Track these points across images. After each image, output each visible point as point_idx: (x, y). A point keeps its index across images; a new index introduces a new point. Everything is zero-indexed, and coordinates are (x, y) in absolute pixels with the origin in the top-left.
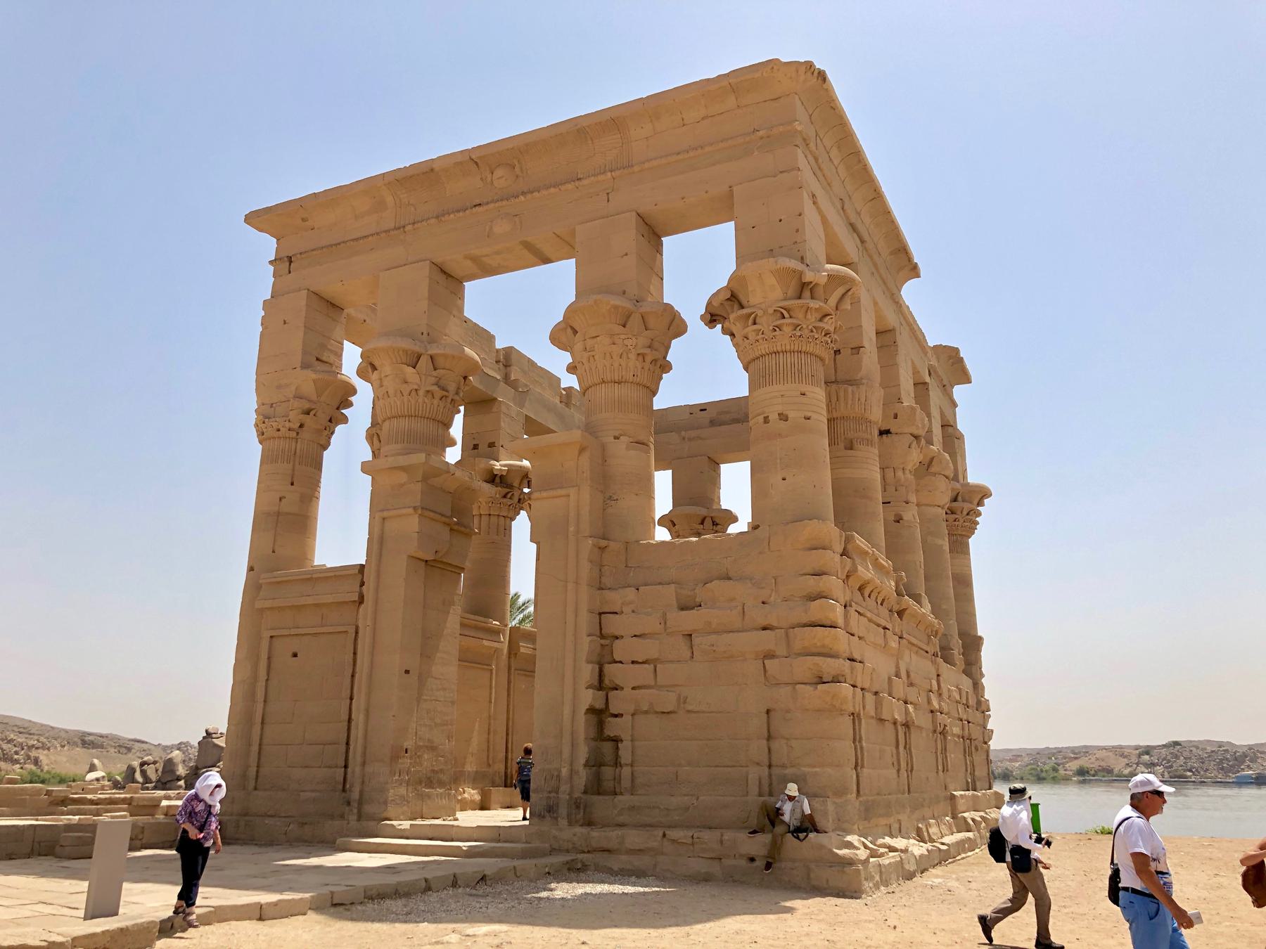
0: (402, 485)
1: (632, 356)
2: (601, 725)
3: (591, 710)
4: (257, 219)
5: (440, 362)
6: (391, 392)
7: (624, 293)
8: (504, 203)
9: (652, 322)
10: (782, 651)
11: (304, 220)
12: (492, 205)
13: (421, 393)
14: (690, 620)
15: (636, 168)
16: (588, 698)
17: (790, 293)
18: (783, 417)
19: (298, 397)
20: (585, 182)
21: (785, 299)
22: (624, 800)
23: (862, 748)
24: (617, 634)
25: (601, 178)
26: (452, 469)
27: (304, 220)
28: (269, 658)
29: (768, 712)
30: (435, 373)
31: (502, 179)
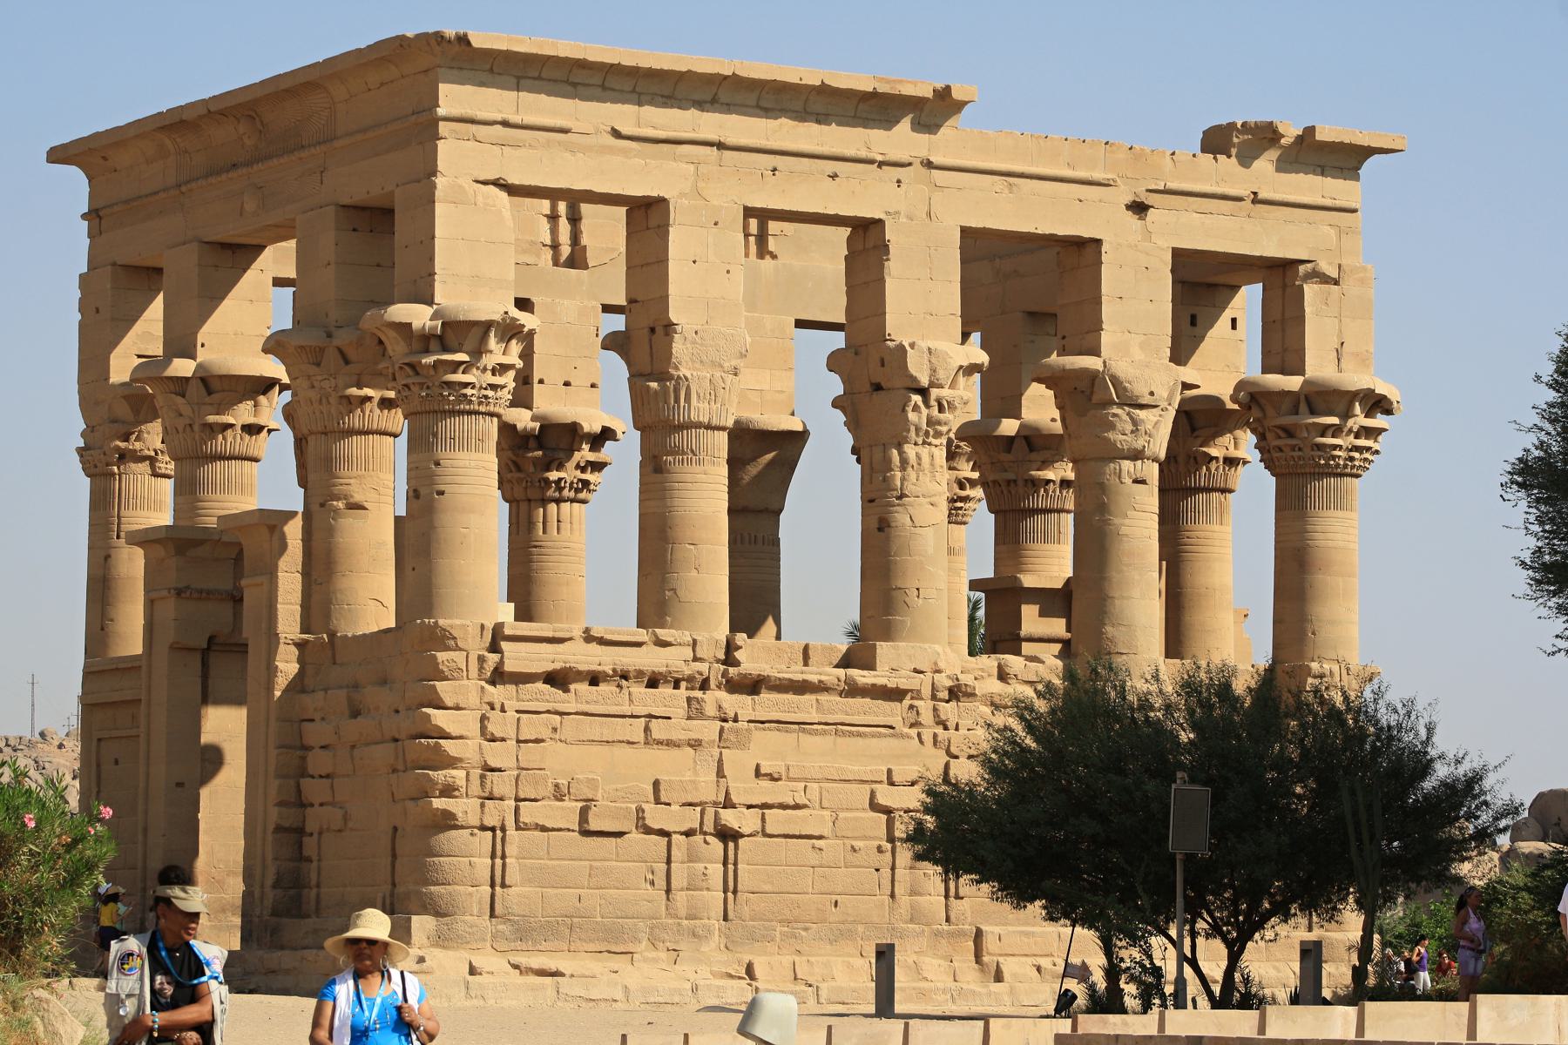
2: (300, 846)
3: (279, 829)
4: (58, 155)
5: (215, 385)
9: (352, 354)
10: (401, 767)
11: (105, 158)
13: (196, 428)
14: (353, 729)
15: (337, 144)
16: (274, 814)
17: (416, 345)
19: (114, 421)
20: (304, 154)
21: (412, 353)
22: (311, 922)
23: (504, 865)
28: (98, 765)
29: (395, 829)
30: (208, 399)
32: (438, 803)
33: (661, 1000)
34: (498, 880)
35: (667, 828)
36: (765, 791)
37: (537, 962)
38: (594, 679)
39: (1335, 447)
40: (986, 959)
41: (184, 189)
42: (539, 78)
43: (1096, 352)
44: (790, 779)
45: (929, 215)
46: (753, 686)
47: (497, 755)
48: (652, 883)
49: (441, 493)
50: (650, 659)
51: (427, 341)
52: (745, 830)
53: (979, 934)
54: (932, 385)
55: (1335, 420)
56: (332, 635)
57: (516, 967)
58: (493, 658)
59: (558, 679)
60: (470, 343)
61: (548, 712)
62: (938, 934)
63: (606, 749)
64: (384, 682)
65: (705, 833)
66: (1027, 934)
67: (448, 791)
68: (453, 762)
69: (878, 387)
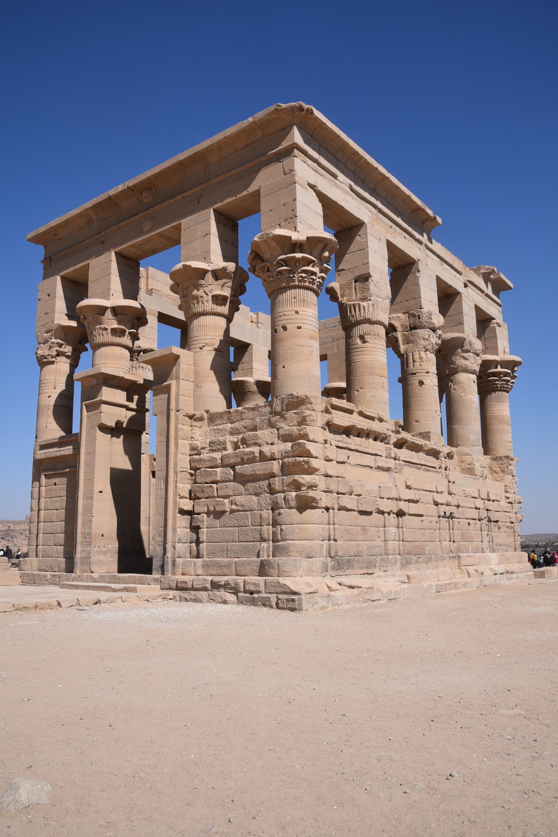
0: (95, 386)
8: (148, 212)
11: (56, 235)
12: (141, 215)
15: (212, 182)
20: (186, 194)
25: (194, 190)
27: (56, 235)
31: (147, 197)
32: (311, 493)
33: (393, 597)
34: (332, 538)
35: (385, 510)
36: (410, 494)
37: (346, 580)
38: (361, 433)
39: (509, 381)
40: (463, 568)
41: (103, 233)
42: (326, 149)
43: (463, 332)
44: (415, 489)
45: (427, 265)
46: (399, 445)
47: (332, 469)
48: (379, 537)
49: (299, 328)
50: (375, 426)
51: (296, 246)
52: (406, 511)
53: (459, 557)
54: (439, 328)
55: (509, 371)
57: (340, 584)
58: (328, 416)
59: (348, 431)
60: (316, 251)
61: (345, 448)
62: (450, 557)
63: (363, 469)
65: (393, 513)
66: (469, 556)
67: (312, 487)
68: (312, 471)
69: (414, 328)
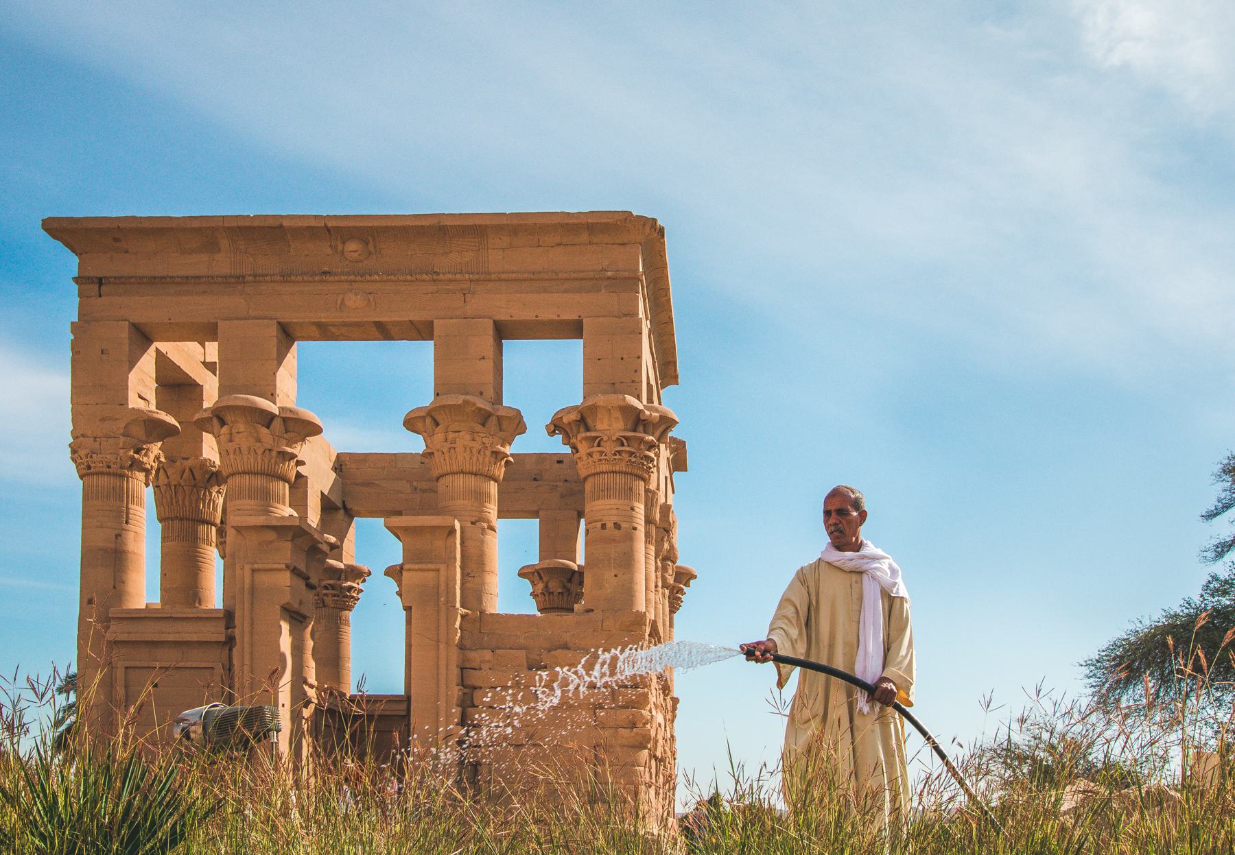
1: (488, 453)
6: (244, 449)
7: (481, 393)
17: (629, 426)
18: (617, 526)
24: (477, 684)
26: (312, 532)
56: (482, 612)
64: (566, 647)
